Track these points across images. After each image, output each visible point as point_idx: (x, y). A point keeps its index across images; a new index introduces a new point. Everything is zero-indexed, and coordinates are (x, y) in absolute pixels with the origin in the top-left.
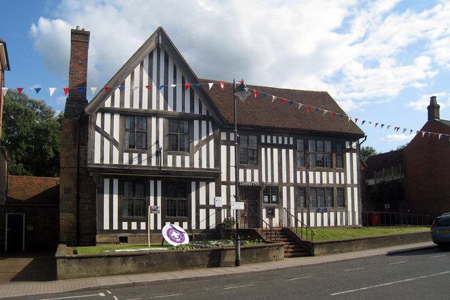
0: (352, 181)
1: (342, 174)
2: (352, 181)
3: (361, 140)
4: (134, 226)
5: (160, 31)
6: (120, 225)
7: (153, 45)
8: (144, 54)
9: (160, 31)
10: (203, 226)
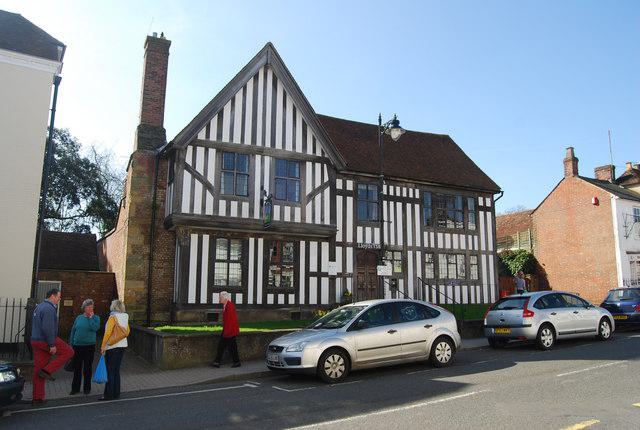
0: (487, 247)
1: (476, 238)
2: (487, 247)
3: (496, 196)
4: (281, 299)
5: (270, 45)
6: (265, 298)
7: (262, 61)
8: (257, 66)
9: (270, 45)
10: (486, 301)
